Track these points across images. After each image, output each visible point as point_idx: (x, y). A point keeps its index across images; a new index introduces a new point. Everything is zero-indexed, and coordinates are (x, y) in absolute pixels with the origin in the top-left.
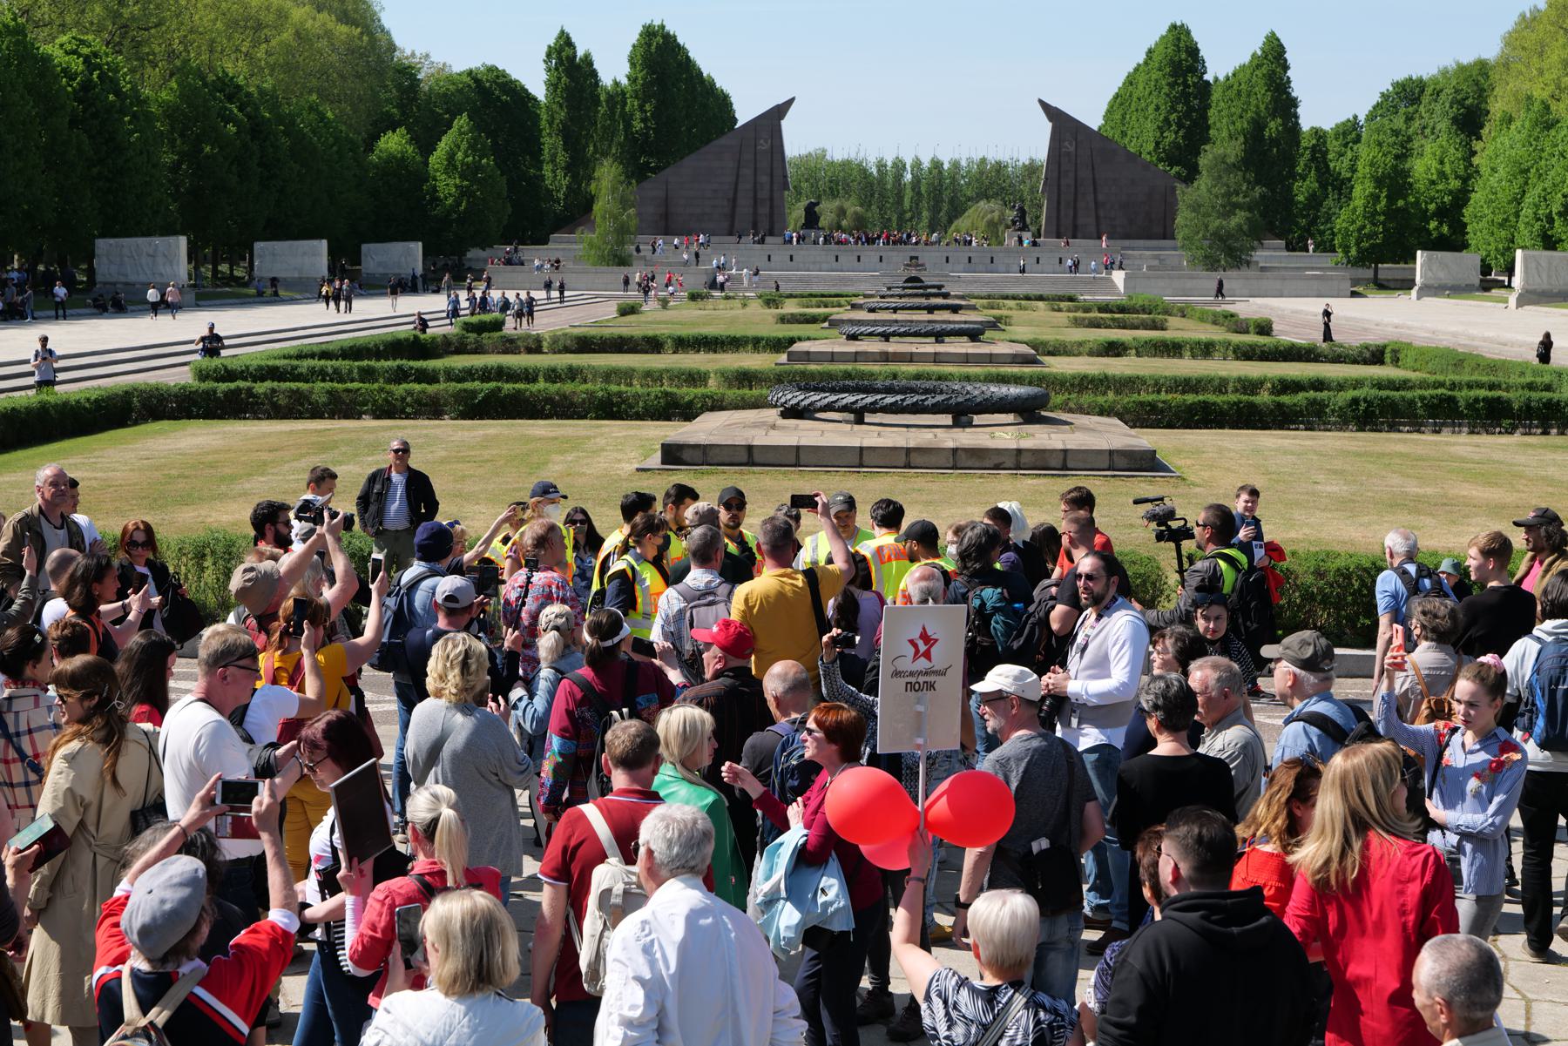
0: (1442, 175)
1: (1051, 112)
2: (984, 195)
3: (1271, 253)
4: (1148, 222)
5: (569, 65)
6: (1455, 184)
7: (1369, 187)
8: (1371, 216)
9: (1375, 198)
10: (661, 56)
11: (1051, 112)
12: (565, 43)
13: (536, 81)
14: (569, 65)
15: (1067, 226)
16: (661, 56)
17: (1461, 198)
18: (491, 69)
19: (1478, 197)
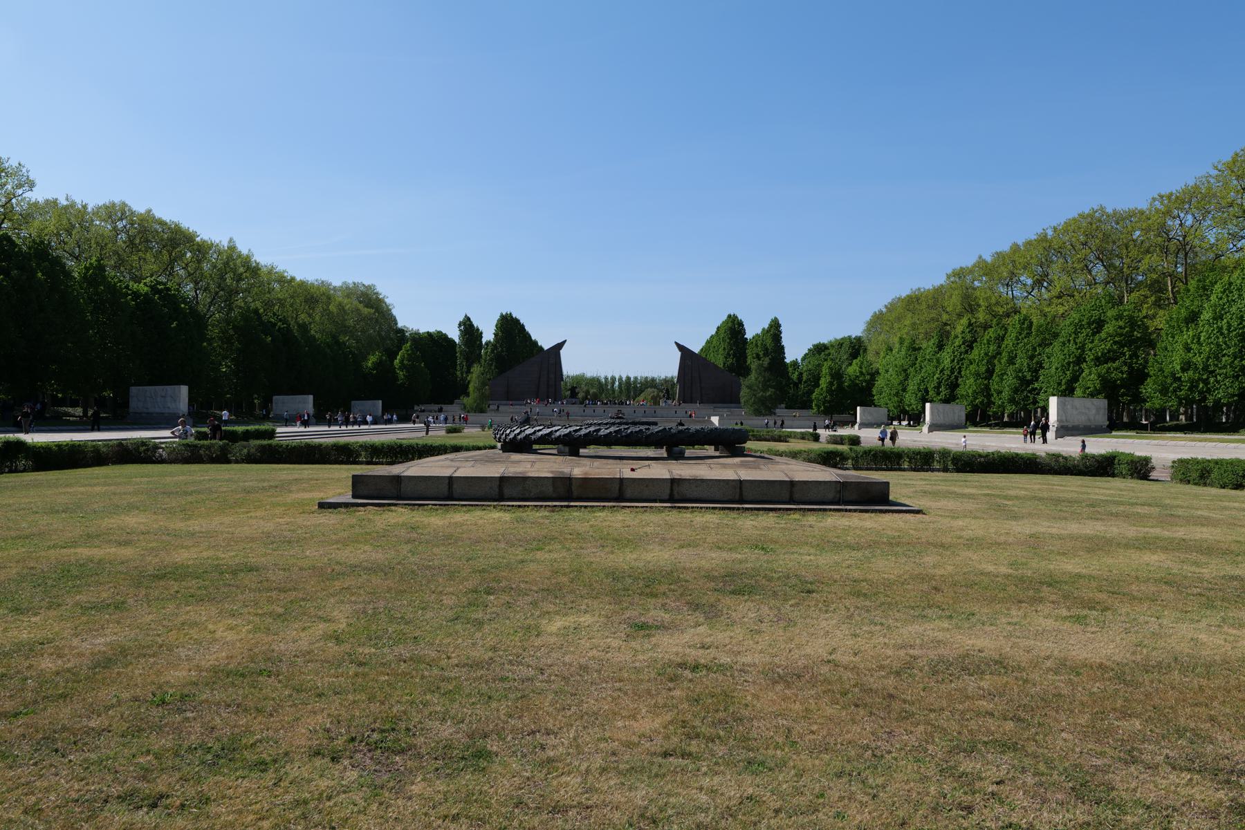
0: (861, 373)
1: (681, 348)
2: (651, 387)
3: (781, 411)
4: (726, 398)
5: (468, 328)
6: (868, 377)
7: (828, 379)
8: (829, 391)
9: (831, 384)
10: (510, 327)
11: (681, 348)
12: (468, 319)
13: (454, 334)
14: (468, 328)
15: (687, 398)
16: (510, 327)
17: (871, 383)
18: (440, 332)
19: (880, 382)
